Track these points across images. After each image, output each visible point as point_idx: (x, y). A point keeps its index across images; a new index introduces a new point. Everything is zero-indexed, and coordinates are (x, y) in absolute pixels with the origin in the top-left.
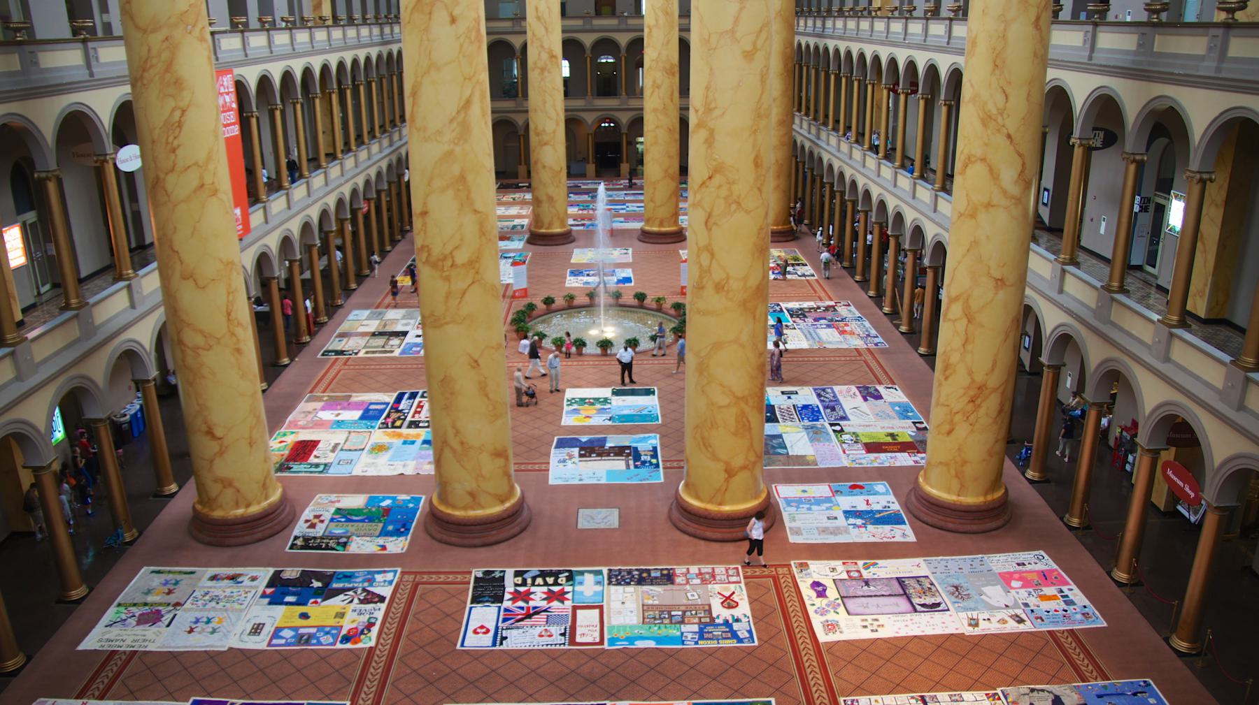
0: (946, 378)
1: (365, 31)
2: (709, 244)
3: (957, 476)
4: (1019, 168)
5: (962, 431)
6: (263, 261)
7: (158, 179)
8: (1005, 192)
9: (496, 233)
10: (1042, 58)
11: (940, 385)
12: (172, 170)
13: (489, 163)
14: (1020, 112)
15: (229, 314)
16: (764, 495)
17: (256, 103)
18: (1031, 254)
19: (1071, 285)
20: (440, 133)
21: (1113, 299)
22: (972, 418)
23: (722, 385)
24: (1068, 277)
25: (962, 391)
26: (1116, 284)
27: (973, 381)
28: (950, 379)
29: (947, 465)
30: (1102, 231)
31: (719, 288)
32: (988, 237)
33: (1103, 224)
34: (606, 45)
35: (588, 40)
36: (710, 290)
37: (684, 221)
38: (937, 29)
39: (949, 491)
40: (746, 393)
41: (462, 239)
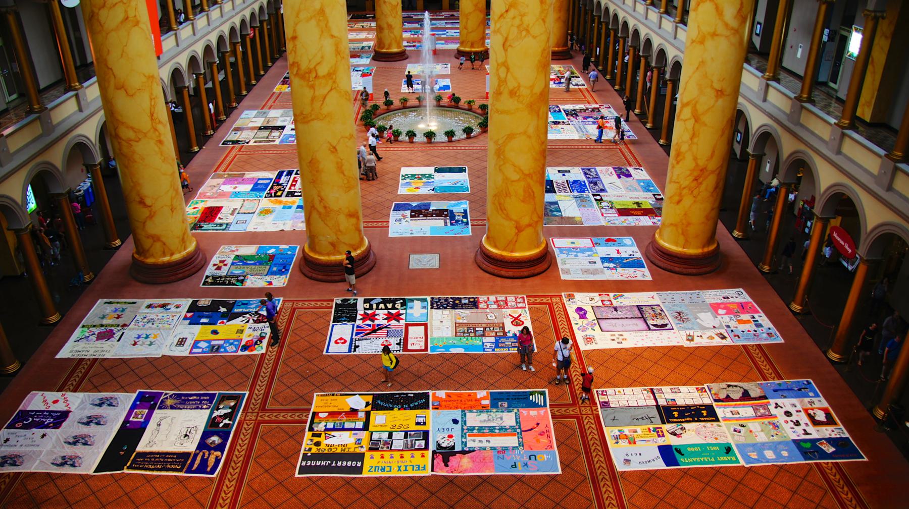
0: (678, 163)
2: (506, 61)
3: (683, 234)
4: (738, 6)
5: (687, 201)
6: (176, 74)
7: (93, 12)
8: (726, 25)
11: (673, 167)
12: (104, 6)
15: (152, 115)
16: (543, 246)
18: (744, 71)
19: (773, 96)
21: (802, 107)
22: (695, 192)
23: (514, 165)
24: (771, 90)
25: (688, 173)
26: (805, 96)
27: (697, 165)
28: (681, 163)
29: (675, 225)
30: (799, 55)
31: (512, 93)
32: (712, 58)
33: (800, 50)
36: (505, 95)
39: (677, 245)
40: (532, 171)
41: (322, 57)
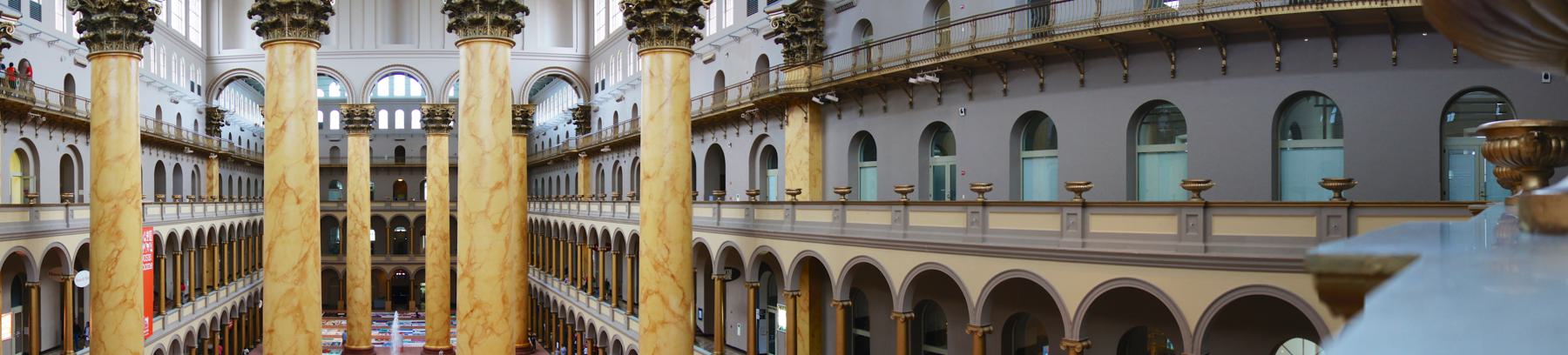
1: (239, 206)
9: (320, 348)
10: (689, 225)
13: (318, 298)
14: (679, 261)
17: (166, 250)
20: (285, 276)
37: (454, 341)
38: (621, 208)
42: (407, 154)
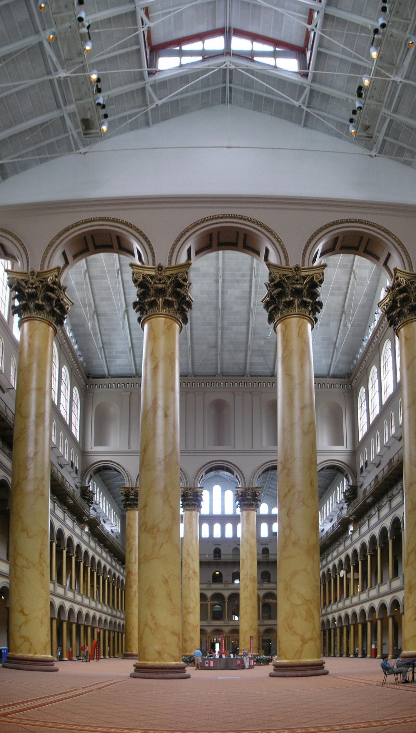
15: (41, 554)
34: (218, 597)
35: (209, 594)
42: (222, 552)
